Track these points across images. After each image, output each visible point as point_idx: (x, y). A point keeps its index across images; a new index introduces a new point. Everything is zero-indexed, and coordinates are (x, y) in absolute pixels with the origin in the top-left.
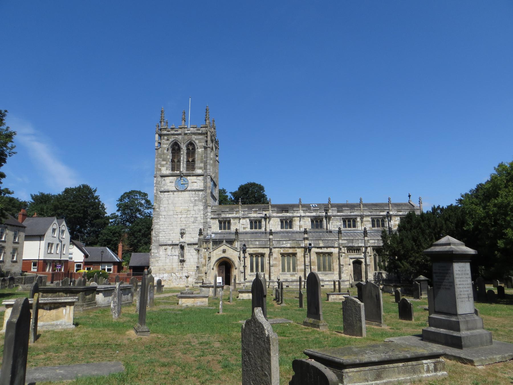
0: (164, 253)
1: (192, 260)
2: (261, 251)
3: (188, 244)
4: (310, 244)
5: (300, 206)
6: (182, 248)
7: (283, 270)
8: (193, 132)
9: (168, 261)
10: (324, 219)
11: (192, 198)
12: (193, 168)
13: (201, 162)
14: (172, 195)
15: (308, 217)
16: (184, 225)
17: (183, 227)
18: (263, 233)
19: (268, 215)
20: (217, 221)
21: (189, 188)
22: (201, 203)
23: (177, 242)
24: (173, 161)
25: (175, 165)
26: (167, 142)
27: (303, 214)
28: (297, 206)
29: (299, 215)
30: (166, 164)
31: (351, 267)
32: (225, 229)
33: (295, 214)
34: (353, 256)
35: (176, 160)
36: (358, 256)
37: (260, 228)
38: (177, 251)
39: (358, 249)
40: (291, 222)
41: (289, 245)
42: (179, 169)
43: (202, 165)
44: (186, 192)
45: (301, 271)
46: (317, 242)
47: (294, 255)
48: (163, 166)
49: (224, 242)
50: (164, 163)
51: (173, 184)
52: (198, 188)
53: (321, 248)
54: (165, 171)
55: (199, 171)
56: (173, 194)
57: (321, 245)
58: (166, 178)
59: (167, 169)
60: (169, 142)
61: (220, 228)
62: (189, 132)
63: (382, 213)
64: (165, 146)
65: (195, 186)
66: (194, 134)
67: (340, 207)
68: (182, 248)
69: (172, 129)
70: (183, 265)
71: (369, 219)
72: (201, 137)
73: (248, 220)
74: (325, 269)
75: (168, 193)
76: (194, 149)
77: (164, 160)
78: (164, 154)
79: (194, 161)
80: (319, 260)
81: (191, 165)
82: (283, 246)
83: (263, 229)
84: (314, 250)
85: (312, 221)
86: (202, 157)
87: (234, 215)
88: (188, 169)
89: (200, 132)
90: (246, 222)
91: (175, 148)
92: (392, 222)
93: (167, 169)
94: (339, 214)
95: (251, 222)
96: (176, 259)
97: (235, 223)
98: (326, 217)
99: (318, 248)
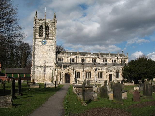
0: (37, 70)
1: (48, 73)
2: (79, 70)
3: (47, 67)
4: (96, 68)
5: (89, 54)
6: (44, 68)
7: (86, 77)
8: (49, 22)
9: (39, 73)
10: (97, 59)
11: (48, 49)
12: (48, 37)
13: (52, 34)
14: (40, 47)
15: (92, 57)
16: (45, 59)
17: (45, 60)
18: (75, 63)
19: (77, 56)
20: (58, 58)
21: (47, 44)
22: (52, 51)
23: (43, 66)
24: (40, 33)
27: (90, 57)
28: (88, 53)
29: (88, 57)
30: (38, 34)
31: (109, 77)
32: (61, 61)
33: (87, 57)
34: (110, 73)
35: (41, 33)
36: (111, 72)
37: (74, 61)
38: (42, 70)
39: (111, 71)
40: (85, 60)
41: (89, 68)
42: (42, 36)
43: (52, 35)
44: (46, 46)
45: (93, 77)
46: (99, 67)
47: (90, 72)
48: (37, 34)
49: (68, 67)
50: (37, 33)
51: (41, 42)
52: (51, 45)
53: (99, 69)
54: (37, 37)
55: (51, 38)
56: (41, 46)
57: (100, 68)
58: (38, 40)
59: (38, 36)
60: (39, 25)
61: (59, 61)
62: (47, 21)
63: (116, 57)
64: (37, 26)
65: (50, 44)
66: (50, 23)
67: (102, 55)
68: (44, 68)
69: (41, 20)
70: (45, 74)
71: (112, 59)
72: (52, 24)
73: (70, 58)
74: (100, 77)
76: (49, 29)
77: (37, 32)
78: (37, 30)
79: (49, 33)
80: (98, 74)
81: (47, 35)
82: (87, 68)
83: (75, 62)
84: (98, 70)
85: (93, 60)
86: (53, 32)
87: (65, 56)
88: (46, 36)
89: (52, 22)
90: (69, 59)
92: (119, 61)
93: (38, 36)
94: (102, 57)
95: (71, 59)
96: (42, 72)
97: (65, 59)
98: (98, 58)
99: (99, 69)
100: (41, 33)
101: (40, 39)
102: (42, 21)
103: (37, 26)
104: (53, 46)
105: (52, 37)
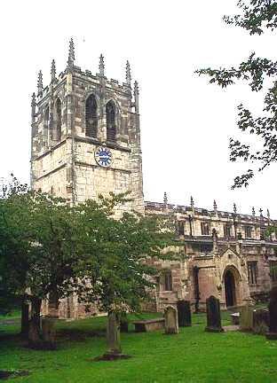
10: (233, 226)
12: (115, 140)
13: (127, 133)
25: (91, 130)
26: (82, 90)
43: (127, 137)
48: (77, 124)
52: (124, 168)
55: (124, 145)
58: (81, 144)
64: (79, 95)
65: (120, 165)
75: (85, 168)
91: (91, 104)
93: (83, 131)
100: (91, 122)
101: (91, 142)
102: (95, 81)
103: (79, 95)
104: (129, 172)
105: (125, 141)
